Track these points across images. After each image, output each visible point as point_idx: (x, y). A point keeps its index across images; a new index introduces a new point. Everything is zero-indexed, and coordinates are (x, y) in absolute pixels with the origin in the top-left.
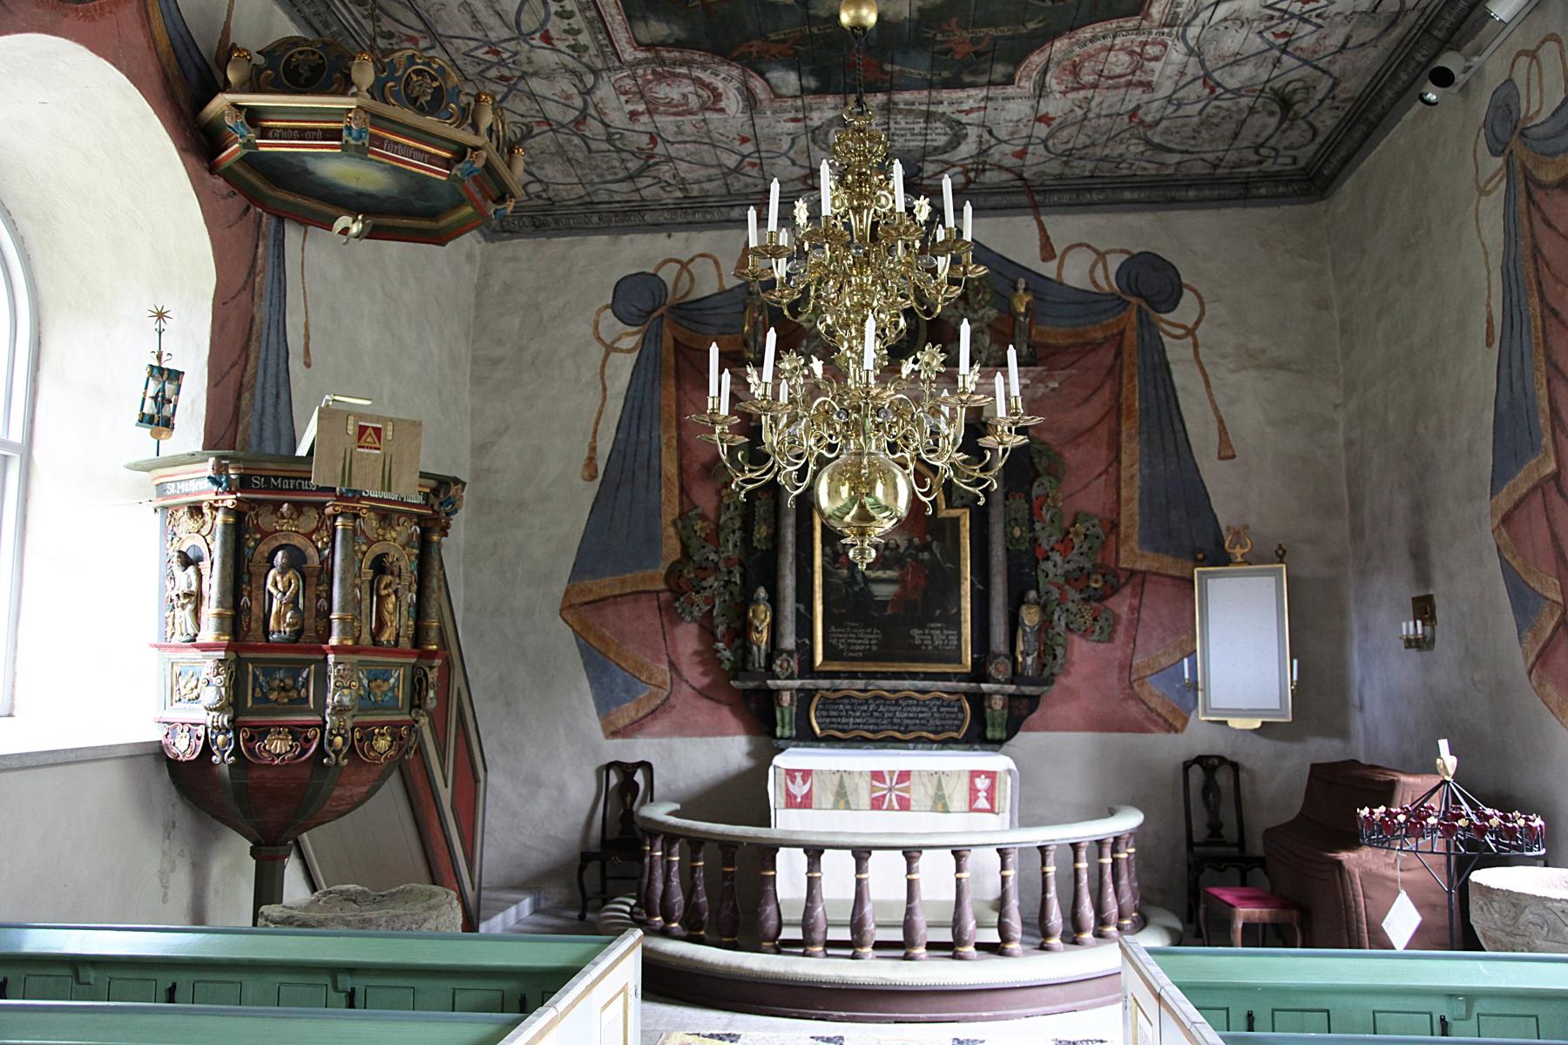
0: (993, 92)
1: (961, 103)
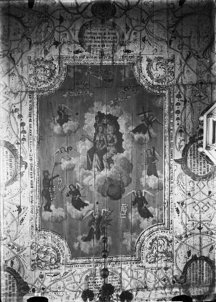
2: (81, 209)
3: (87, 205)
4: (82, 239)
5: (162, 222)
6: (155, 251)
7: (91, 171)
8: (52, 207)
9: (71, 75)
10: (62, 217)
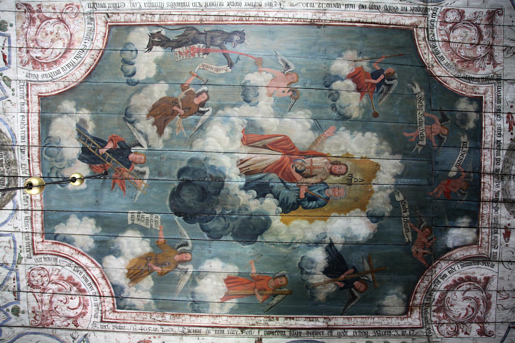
0: (489, 107)
1: (500, 129)
2: (152, 120)
3: (160, 132)
4: (83, 121)
5: (119, 308)
6: (54, 287)
7: (239, 143)
8: (158, 51)
9: (462, 105)
10: (134, 74)
